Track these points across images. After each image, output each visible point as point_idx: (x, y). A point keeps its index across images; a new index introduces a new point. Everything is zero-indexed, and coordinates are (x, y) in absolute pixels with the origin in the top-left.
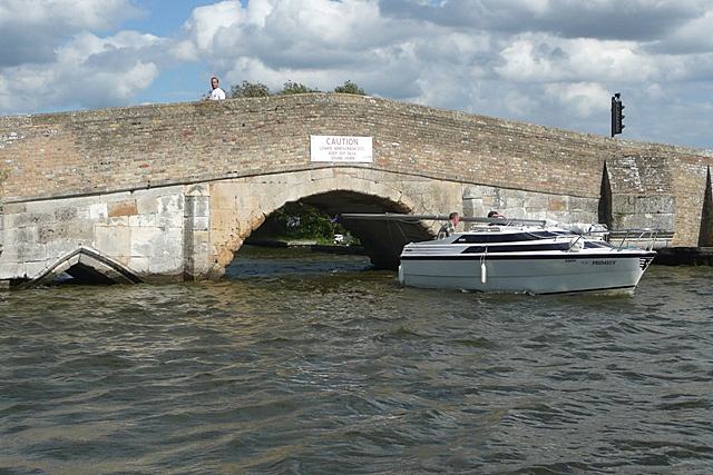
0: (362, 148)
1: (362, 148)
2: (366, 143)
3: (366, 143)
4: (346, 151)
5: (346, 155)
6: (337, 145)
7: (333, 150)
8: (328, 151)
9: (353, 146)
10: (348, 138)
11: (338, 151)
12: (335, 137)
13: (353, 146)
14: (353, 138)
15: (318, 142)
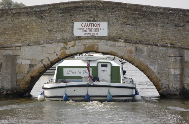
0: (103, 29)
1: (103, 29)
2: (104, 25)
3: (104, 25)
4: (93, 30)
5: (93, 32)
6: (87, 27)
7: (85, 29)
8: (82, 30)
9: (97, 27)
10: (94, 23)
11: (88, 30)
12: (87, 23)
13: (97, 27)
14: (97, 23)
15: (77, 25)
